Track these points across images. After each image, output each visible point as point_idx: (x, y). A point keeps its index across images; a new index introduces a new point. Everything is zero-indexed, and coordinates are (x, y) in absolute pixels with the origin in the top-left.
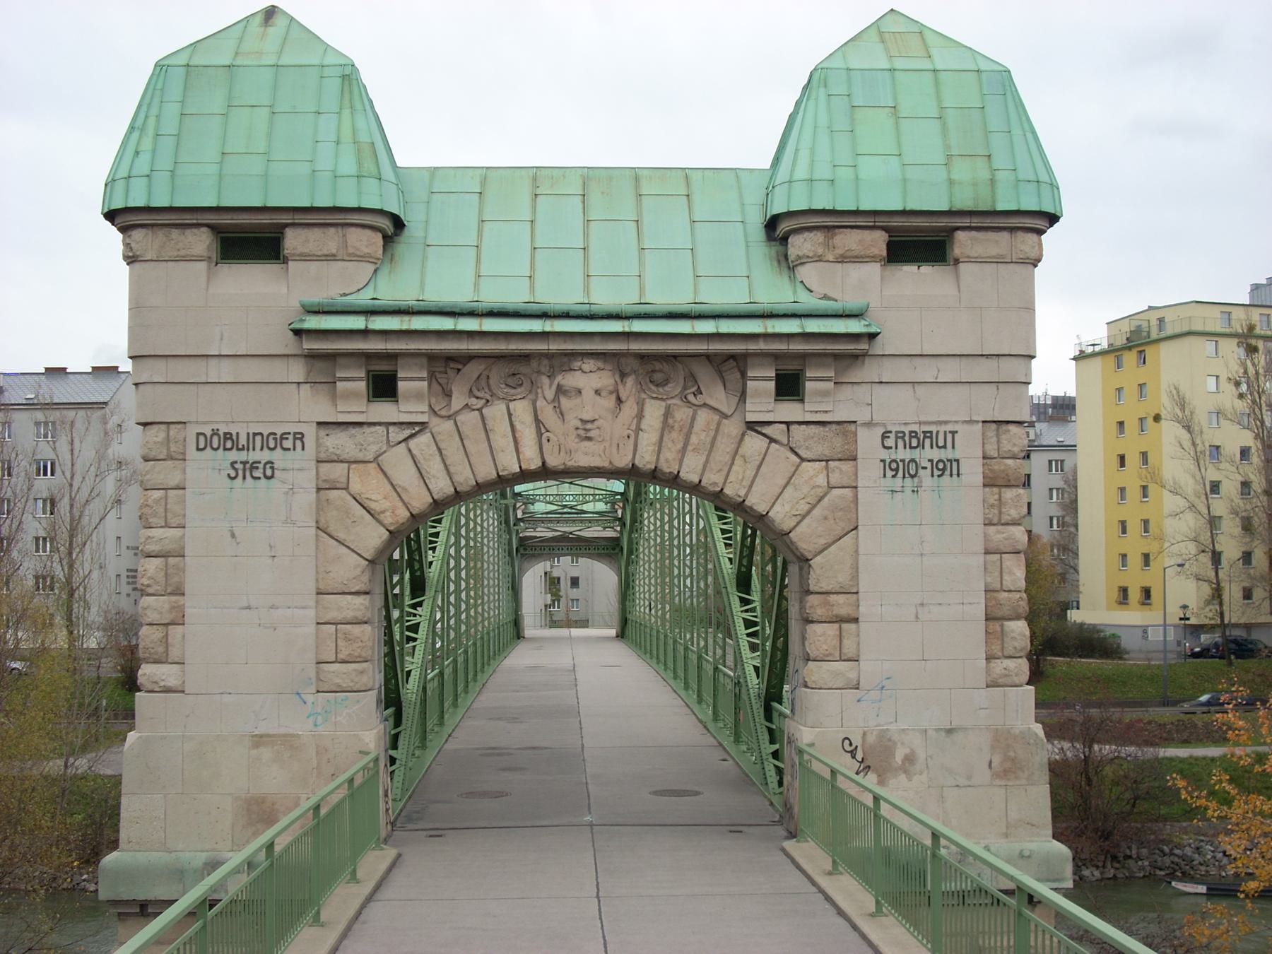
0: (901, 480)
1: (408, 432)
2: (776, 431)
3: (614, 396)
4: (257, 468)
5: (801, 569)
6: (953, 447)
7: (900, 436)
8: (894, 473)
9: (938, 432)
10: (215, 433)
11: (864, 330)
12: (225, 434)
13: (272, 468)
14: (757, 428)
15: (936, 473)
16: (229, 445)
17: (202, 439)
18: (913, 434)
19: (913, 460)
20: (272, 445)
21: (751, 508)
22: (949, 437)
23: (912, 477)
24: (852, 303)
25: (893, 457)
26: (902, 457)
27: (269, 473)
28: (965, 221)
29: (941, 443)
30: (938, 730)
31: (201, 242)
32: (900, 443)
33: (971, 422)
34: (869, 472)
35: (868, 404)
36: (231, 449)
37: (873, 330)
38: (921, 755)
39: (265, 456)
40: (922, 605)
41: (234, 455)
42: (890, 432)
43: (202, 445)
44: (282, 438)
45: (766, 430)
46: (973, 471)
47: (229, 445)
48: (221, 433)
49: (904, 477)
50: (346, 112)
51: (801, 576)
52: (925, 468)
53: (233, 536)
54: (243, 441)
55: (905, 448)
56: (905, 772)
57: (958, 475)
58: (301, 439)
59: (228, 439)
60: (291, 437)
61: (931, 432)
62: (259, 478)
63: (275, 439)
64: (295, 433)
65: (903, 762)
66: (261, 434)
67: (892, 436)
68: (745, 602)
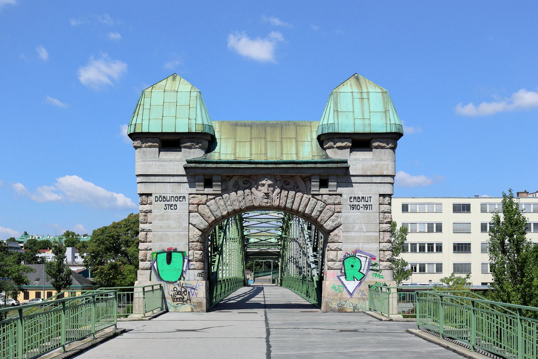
7: (355, 198)
9: (366, 197)
10: (160, 197)
12: (163, 197)
13: (176, 206)
18: (359, 198)
22: (369, 198)
23: (358, 209)
27: (175, 208)
32: (355, 200)
36: (165, 201)
39: (174, 203)
41: (166, 203)
43: (157, 200)
46: (375, 207)
48: (162, 196)
52: (362, 207)
54: (168, 199)
58: (185, 198)
60: (182, 198)
61: (364, 197)
62: (173, 209)
66: (173, 197)
67: (353, 198)
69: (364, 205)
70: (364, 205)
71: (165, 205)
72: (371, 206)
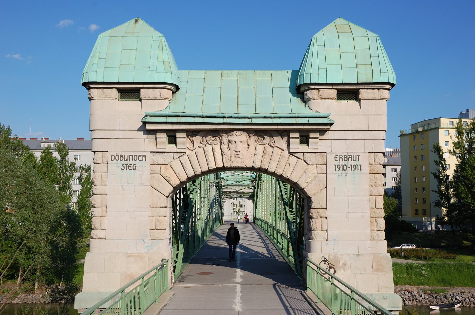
0: (341, 171)
2: (301, 155)
3: (247, 143)
4: (131, 166)
5: (308, 200)
6: (359, 161)
8: (339, 169)
9: (353, 156)
10: (117, 155)
11: (329, 122)
12: (121, 155)
13: (136, 166)
14: (293, 154)
15: (353, 169)
16: (122, 159)
17: (113, 156)
18: (345, 156)
19: (345, 165)
20: (136, 159)
21: (291, 180)
22: (357, 157)
23: (345, 170)
24: (324, 113)
25: (339, 164)
26: (342, 164)
27: (134, 168)
28: (363, 86)
29: (355, 159)
30: (354, 254)
31: (114, 93)
32: (341, 159)
33: (365, 152)
34: (331, 169)
35: (330, 147)
37: (332, 122)
38: (348, 263)
39: (132, 162)
41: (123, 162)
42: (338, 156)
43: (113, 159)
45: (296, 155)
46: (365, 168)
47: (122, 159)
48: (119, 155)
49: (342, 170)
50: (160, 52)
51: (308, 202)
53: (123, 188)
54: (126, 158)
55: (342, 161)
56: (343, 268)
57: (360, 170)
58: (145, 157)
59: (121, 157)
60: (142, 156)
61: (351, 156)
62: (131, 170)
63: (137, 157)
64: (143, 155)
65: (342, 265)
67: (338, 157)
68: (291, 212)
69: (351, 165)
70: (351, 165)
72: (359, 166)
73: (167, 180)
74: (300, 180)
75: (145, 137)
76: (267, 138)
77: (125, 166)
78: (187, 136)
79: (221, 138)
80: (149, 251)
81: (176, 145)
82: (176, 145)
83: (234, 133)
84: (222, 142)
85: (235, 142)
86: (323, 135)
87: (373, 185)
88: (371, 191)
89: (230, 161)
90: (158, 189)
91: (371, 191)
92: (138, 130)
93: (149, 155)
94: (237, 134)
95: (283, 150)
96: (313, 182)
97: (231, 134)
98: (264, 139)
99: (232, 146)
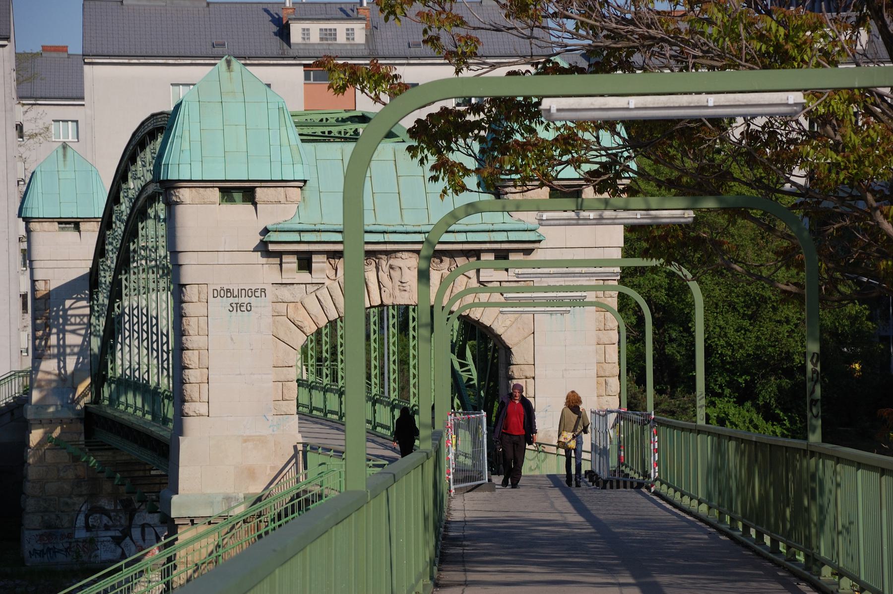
1: (316, 288)
5: (506, 352)
10: (222, 289)
11: (537, 239)
16: (229, 294)
17: (215, 291)
27: (249, 308)
31: (216, 194)
40: (566, 370)
41: (232, 300)
43: (215, 295)
44: (255, 292)
47: (229, 294)
50: (283, 129)
51: (506, 355)
53: (232, 339)
54: (236, 293)
58: (264, 292)
60: (259, 291)
71: (231, 305)
73: (298, 326)
74: (495, 323)
75: (264, 260)
76: (447, 260)
77: (234, 305)
78: (328, 258)
79: (377, 261)
80: (275, 433)
81: (311, 273)
82: (311, 273)
83: (399, 255)
84: (380, 268)
85: (400, 268)
86: (529, 254)
87: (602, 328)
88: (599, 338)
89: (392, 295)
90: (285, 340)
91: (599, 338)
92: (254, 251)
93: (270, 289)
94: (403, 257)
95: (470, 278)
96: (514, 325)
97: (393, 255)
98: (441, 261)
99: (396, 274)
